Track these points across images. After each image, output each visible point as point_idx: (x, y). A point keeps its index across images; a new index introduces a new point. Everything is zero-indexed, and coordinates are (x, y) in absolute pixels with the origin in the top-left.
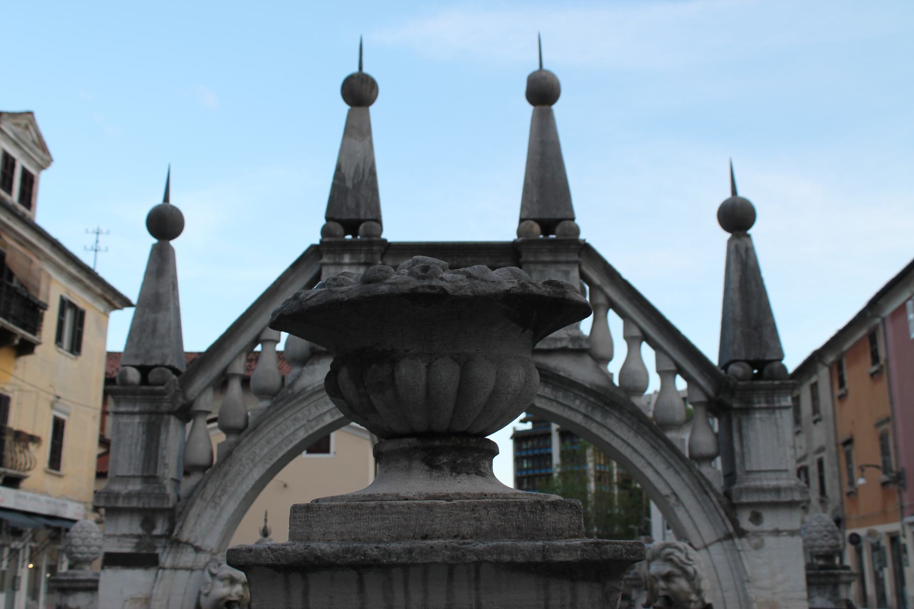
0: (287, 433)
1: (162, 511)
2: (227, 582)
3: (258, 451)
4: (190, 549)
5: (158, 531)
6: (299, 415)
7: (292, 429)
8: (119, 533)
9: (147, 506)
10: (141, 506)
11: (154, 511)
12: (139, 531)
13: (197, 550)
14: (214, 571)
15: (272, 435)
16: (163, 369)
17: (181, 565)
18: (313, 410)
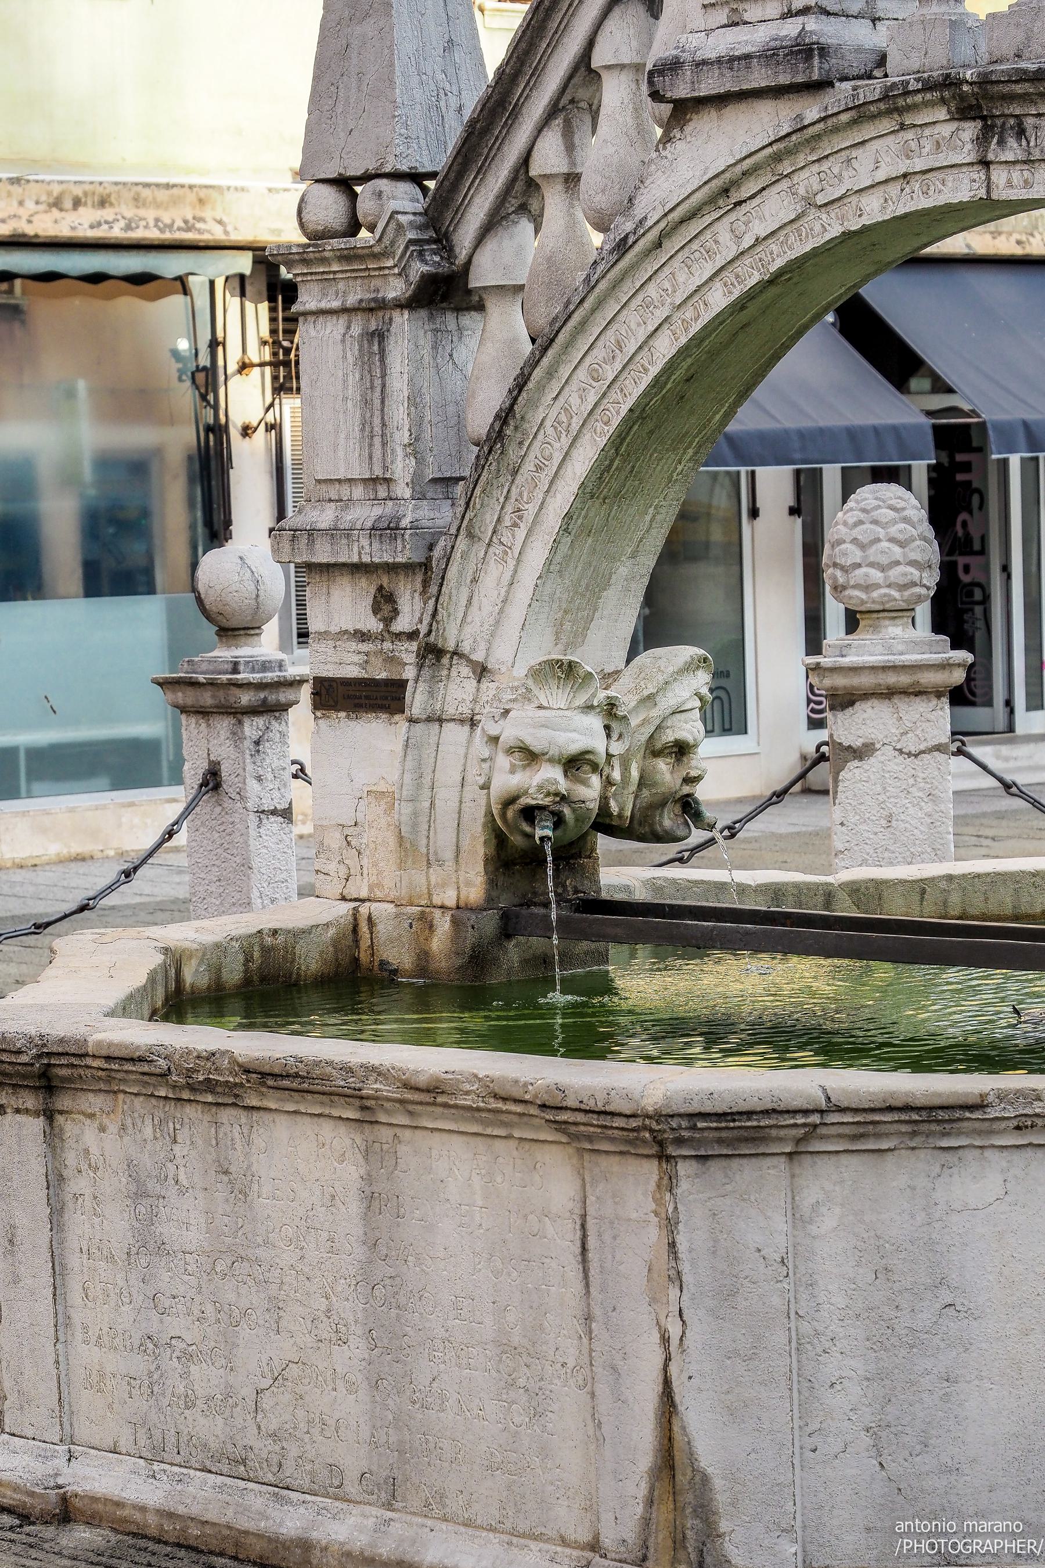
0: (631, 348)
1: (408, 568)
2: (517, 759)
3: (574, 400)
4: (465, 671)
5: (403, 623)
6: (652, 290)
7: (642, 335)
8: (334, 629)
9: (366, 559)
10: (355, 559)
11: (392, 568)
12: (373, 625)
13: (482, 671)
14: (493, 730)
15: (599, 353)
16: (383, 184)
17: (451, 711)
18: (681, 277)
